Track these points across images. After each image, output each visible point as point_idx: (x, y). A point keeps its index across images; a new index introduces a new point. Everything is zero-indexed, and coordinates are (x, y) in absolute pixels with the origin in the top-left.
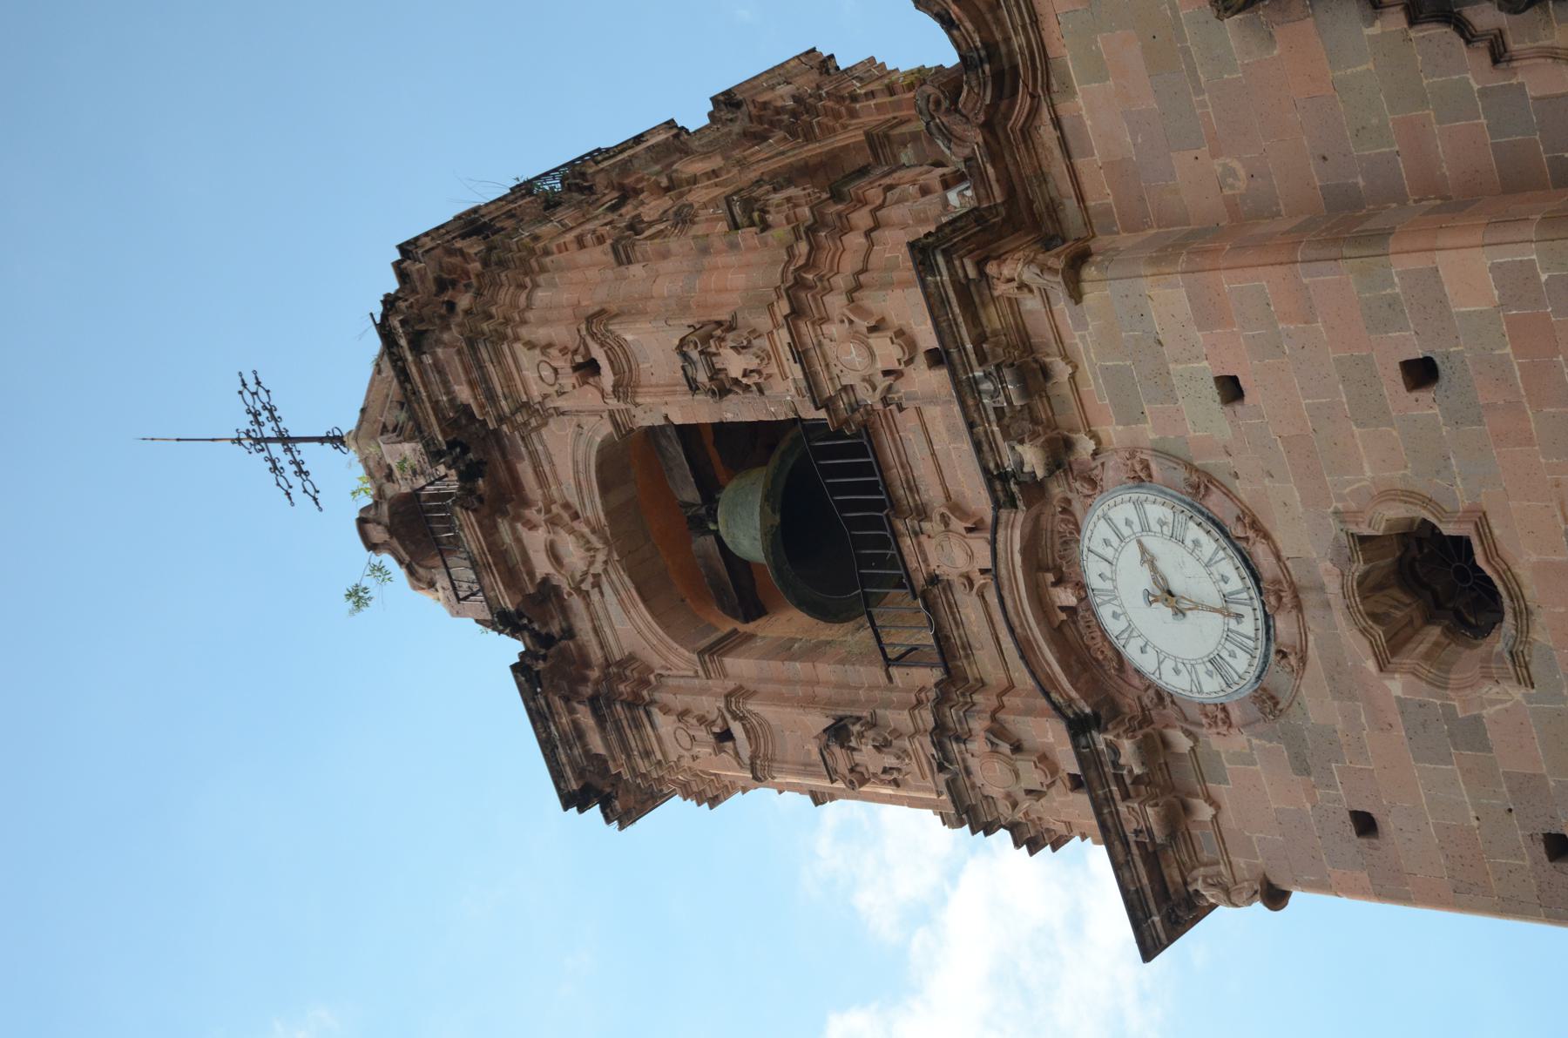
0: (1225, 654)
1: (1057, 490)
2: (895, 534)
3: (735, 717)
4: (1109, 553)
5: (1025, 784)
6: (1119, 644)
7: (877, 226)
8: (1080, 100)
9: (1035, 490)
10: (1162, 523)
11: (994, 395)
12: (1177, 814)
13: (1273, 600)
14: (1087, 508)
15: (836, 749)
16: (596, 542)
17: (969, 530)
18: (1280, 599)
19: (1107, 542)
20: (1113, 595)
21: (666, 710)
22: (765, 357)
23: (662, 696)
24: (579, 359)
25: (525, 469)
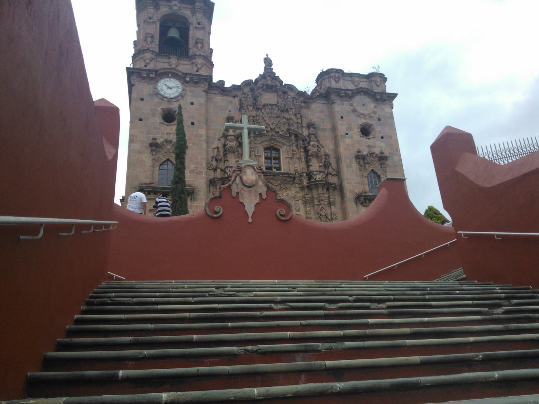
0: (163, 91)
1: (182, 79)
2: (177, 56)
3: (153, 22)
4: (175, 82)
5: (146, 60)
6: (164, 79)
7: (210, 69)
8: (219, 97)
9: (184, 78)
10: (178, 90)
11: (195, 78)
12: (144, 78)
13: (170, 99)
14: (180, 82)
15: (151, 36)
16: (176, 12)
17: (176, 65)
18: (170, 100)
19: (176, 83)
20: (170, 81)
21: (154, 11)
22: (199, 50)
23: (155, 11)
24: (200, 23)
25: (185, 6)
